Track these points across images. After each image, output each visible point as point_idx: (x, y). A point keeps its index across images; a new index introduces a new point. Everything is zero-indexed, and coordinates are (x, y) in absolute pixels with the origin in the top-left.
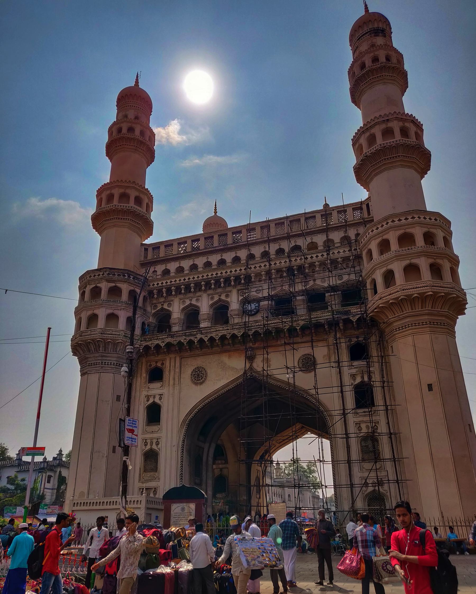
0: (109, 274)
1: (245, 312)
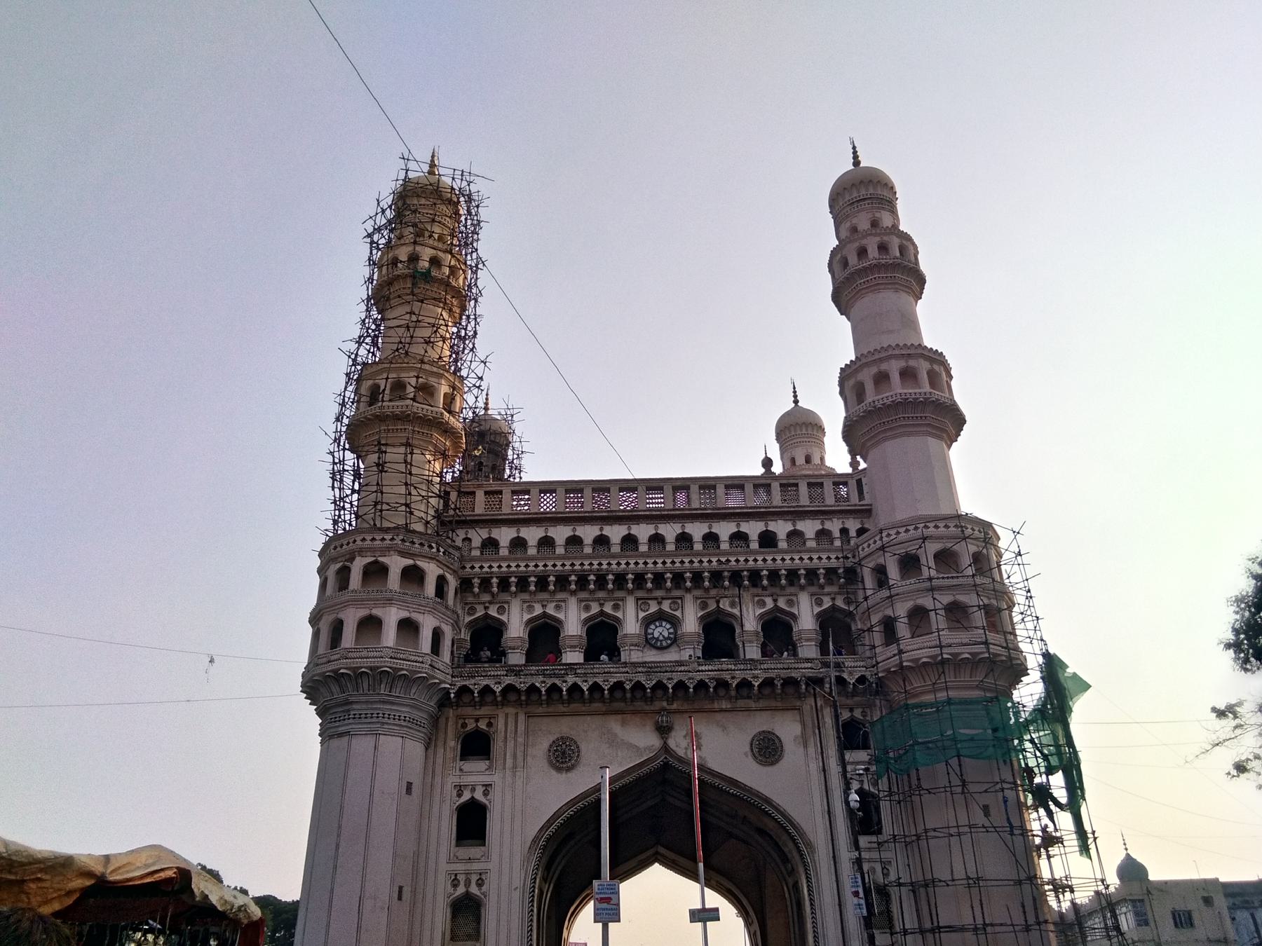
0: (403, 540)
1: (649, 642)
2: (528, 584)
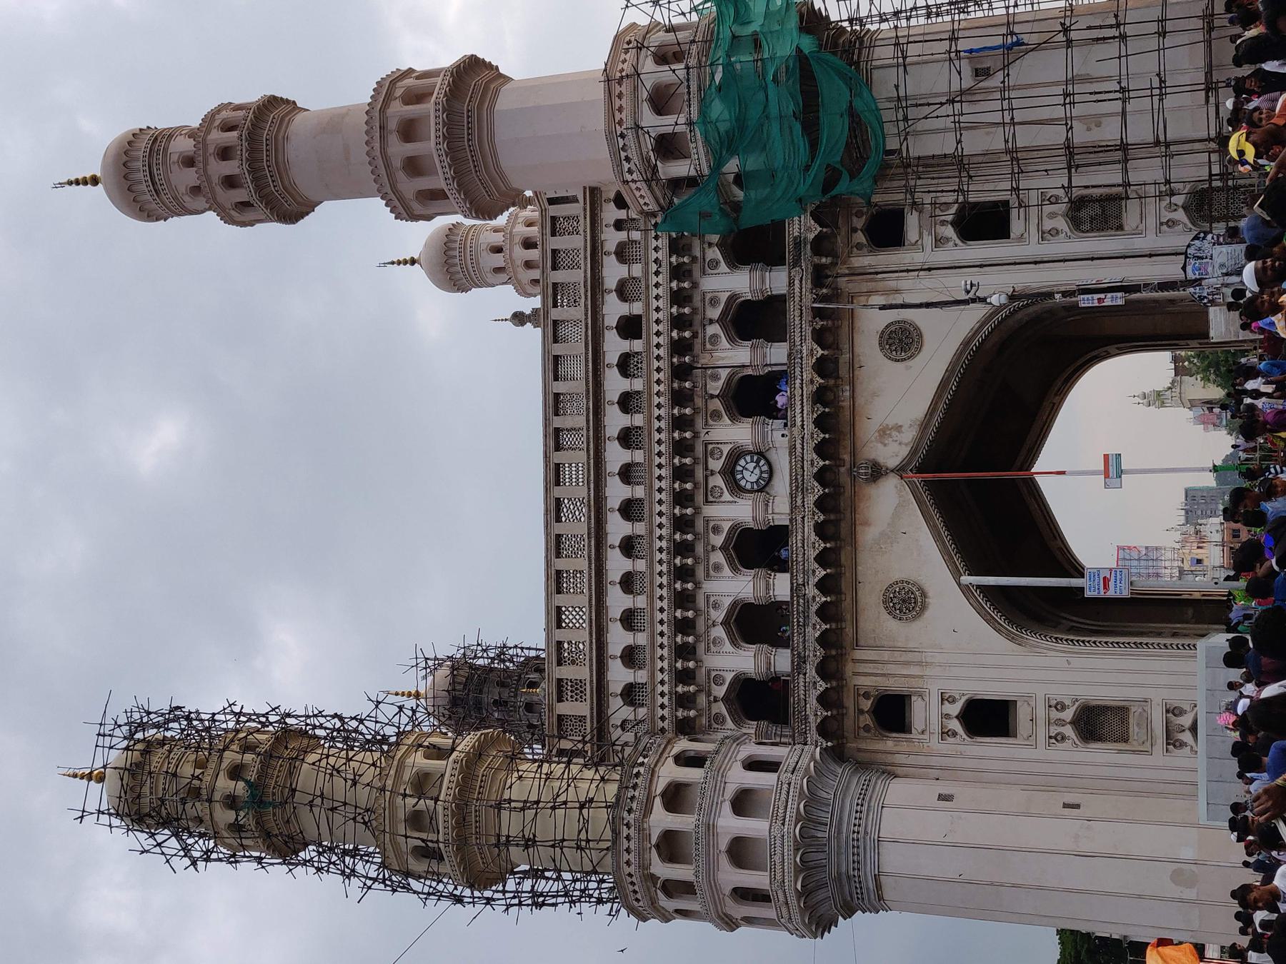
1: (763, 487)
2: (685, 644)
